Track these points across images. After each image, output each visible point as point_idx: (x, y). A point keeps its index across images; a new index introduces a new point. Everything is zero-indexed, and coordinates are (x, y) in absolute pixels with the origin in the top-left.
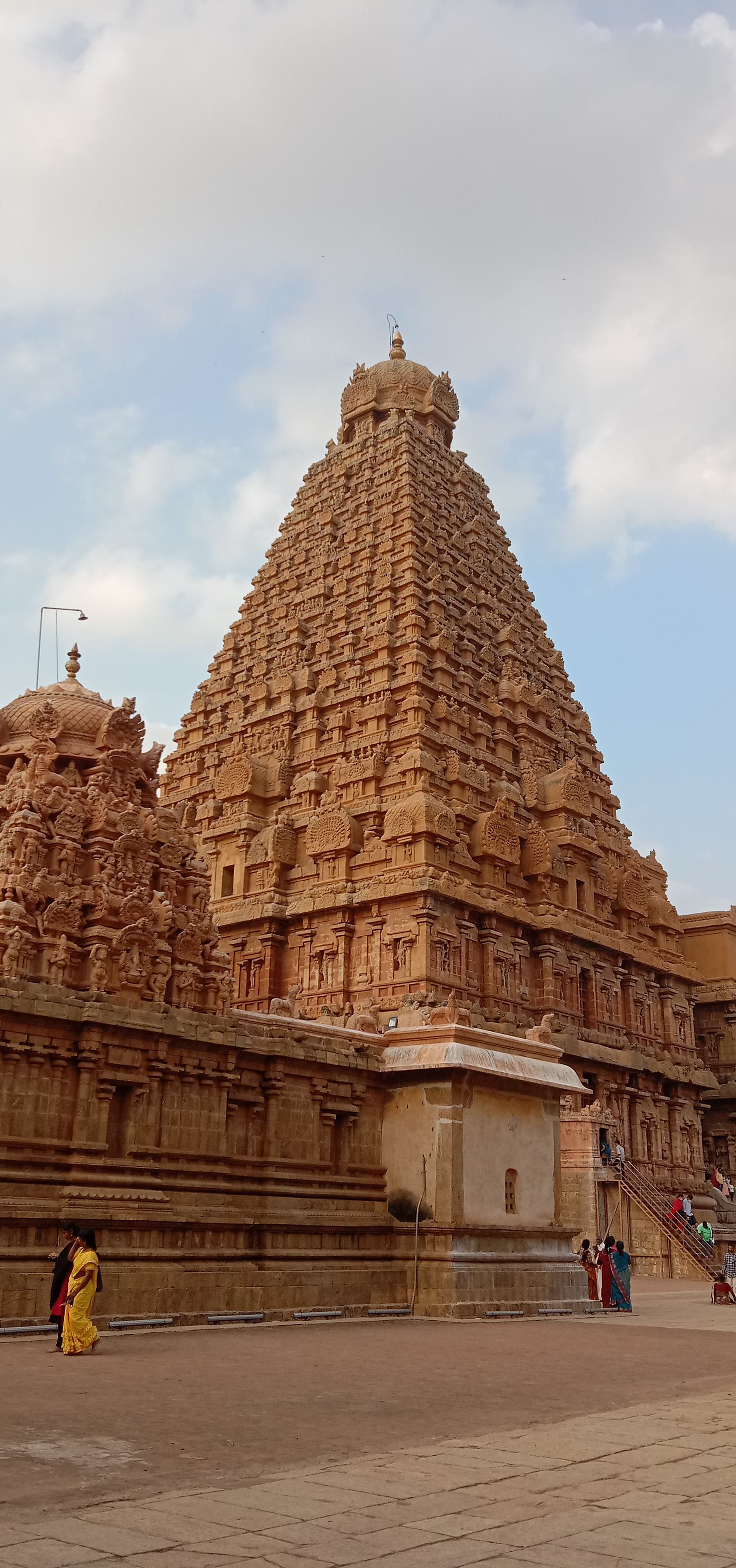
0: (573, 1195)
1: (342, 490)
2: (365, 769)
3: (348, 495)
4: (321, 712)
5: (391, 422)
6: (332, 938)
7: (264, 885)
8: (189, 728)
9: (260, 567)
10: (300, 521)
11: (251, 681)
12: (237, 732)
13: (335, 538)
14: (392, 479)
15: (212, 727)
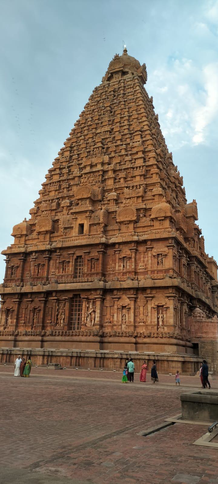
0: (210, 347)
1: (112, 96)
2: (138, 193)
3: (115, 98)
4: (115, 171)
5: (129, 76)
6: (129, 252)
7: (97, 231)
8: (53, 173)
9: (77, 120)
10: (93, 105)
11: (80, 159)
12: (77, 176)
13: (111, 112)
14: (133, 94)
15: (64, 174)
